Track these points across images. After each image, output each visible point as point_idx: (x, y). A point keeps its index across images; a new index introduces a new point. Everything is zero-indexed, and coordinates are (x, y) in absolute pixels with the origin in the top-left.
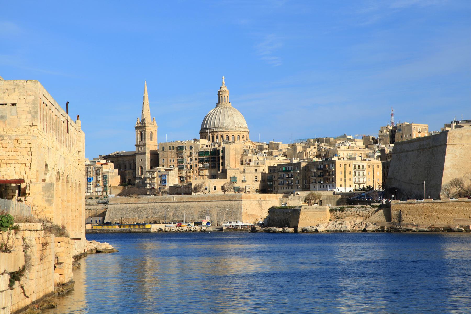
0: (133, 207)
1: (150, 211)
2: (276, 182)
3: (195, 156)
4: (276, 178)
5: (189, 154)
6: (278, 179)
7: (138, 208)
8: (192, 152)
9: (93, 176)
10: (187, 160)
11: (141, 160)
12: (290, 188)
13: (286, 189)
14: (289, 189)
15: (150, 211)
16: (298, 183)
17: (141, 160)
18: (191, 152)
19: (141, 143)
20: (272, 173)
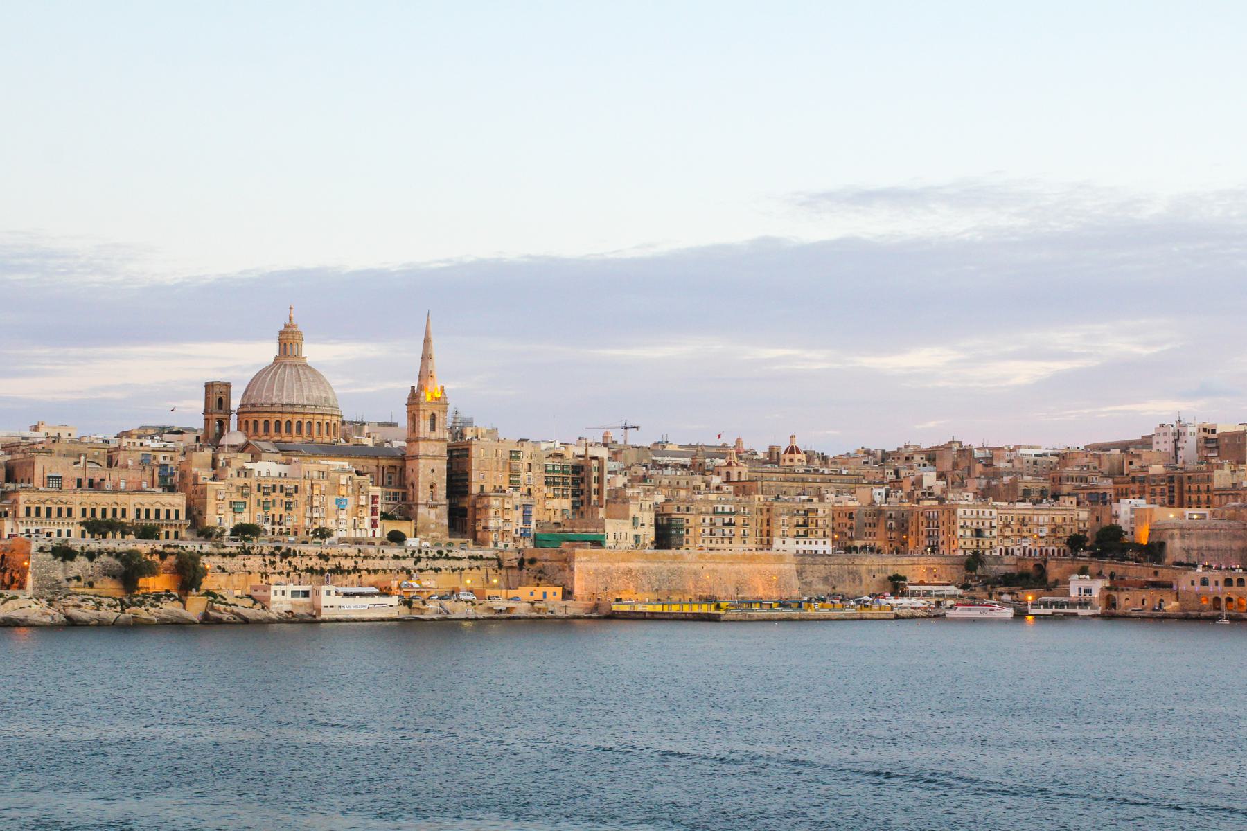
0: (622, 569)
1: (653, 578)
2: (690, 530)
3: (538, 471)
4: (691, 523)
5: (526, 466)
6: (696, 525)
7: (630, 571)
8: (532, 463)
9: (348, 496)
10: (524, 476)
11: (433, 471)
12: (727, 541)
13: (717, 542)
14: (723, 542)
15: (653, 578)
16: (744, 535)
17: (433, 471)
18: (530, 464)
19: (433, 436)
20: (683, 514)
